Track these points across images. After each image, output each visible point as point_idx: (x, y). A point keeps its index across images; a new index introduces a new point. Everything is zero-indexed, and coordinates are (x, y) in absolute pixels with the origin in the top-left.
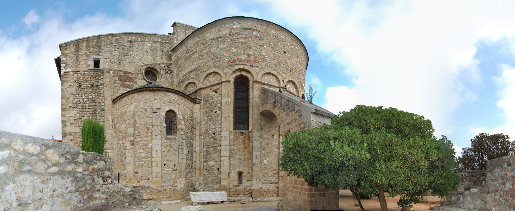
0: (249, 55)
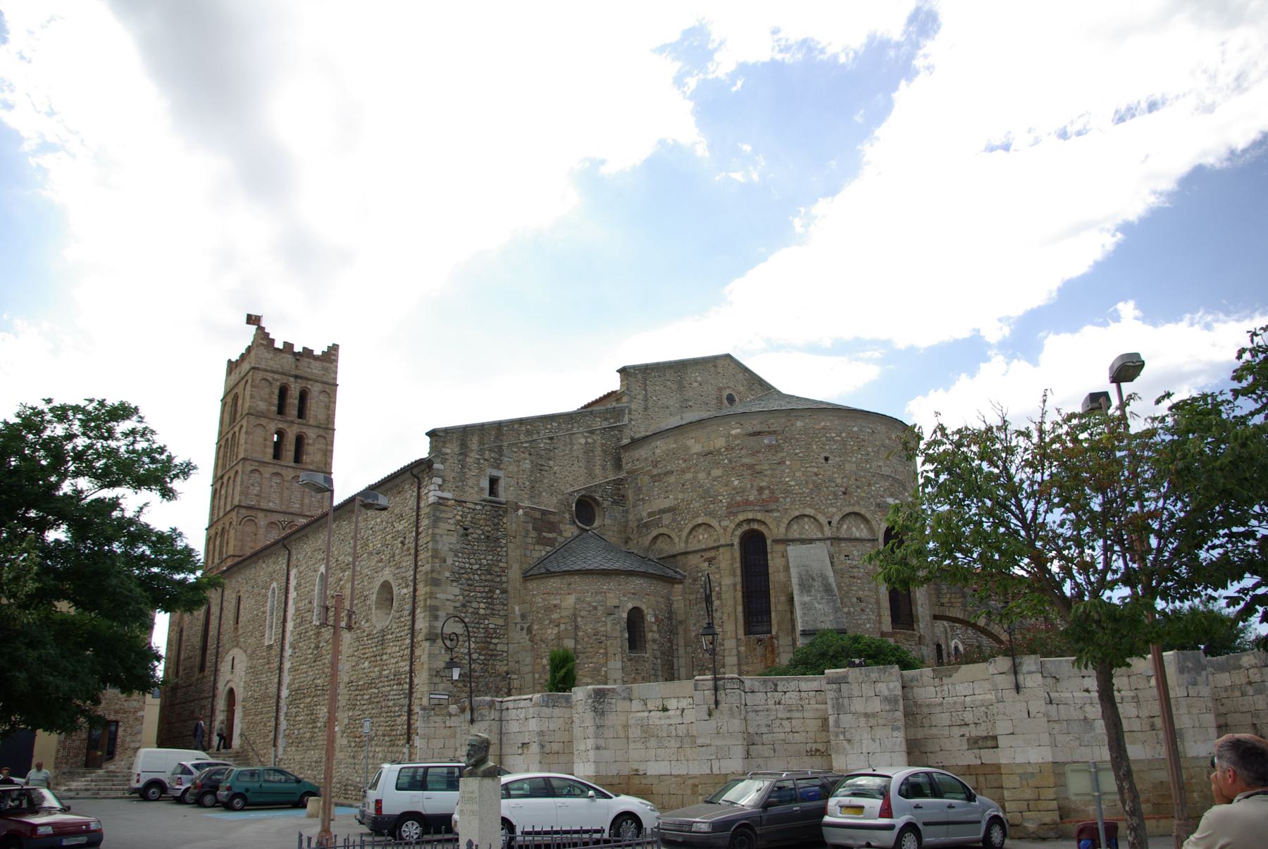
0: (761, 490)
